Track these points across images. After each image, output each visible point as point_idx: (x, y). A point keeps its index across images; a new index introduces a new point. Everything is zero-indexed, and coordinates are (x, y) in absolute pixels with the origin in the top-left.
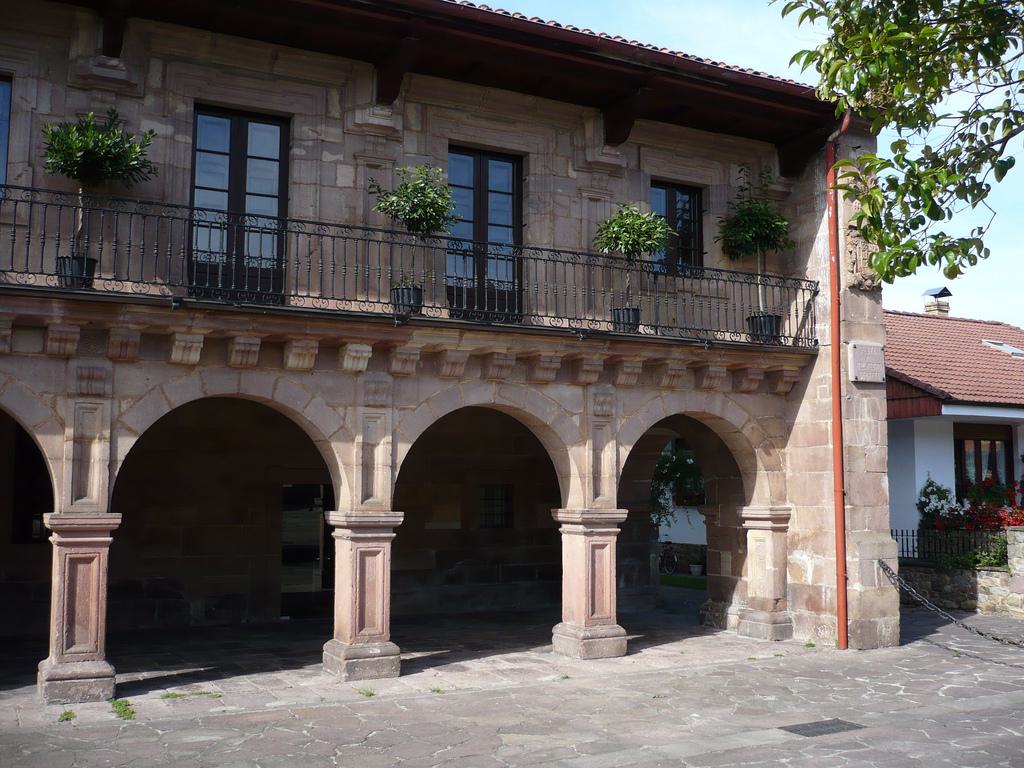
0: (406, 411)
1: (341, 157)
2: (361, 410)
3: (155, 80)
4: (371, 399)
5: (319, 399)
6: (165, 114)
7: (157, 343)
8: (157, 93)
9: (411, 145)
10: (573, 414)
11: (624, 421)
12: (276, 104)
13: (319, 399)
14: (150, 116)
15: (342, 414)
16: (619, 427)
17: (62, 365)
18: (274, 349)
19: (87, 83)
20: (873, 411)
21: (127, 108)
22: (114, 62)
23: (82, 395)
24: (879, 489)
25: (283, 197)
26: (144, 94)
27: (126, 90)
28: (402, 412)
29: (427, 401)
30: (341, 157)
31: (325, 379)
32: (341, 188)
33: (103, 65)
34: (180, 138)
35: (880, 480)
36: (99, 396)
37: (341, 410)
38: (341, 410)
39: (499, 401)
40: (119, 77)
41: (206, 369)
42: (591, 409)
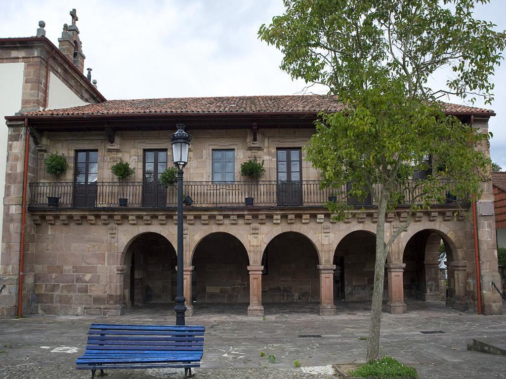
2: (323, 234)
3: (266, 144)
4: (325, 231)
5: (312, 231)
6: (269, 154)
7: (270, 217)
8: (267, 148)
13: (312, 231)
14: (266, 155)
17: (249, 226)
18: (299, 216)
19: (250, 149)
20: (489, 226)
21: (260, 153)
22: (256, 143)
23: (253, 234)
24: (494, 255)
25: (301, 172)
27: (259, 149)
29: (342, 230)
31: (312, 225)
34: (273, 159)
35: (493, 252)
36: (257, 234)
37: (318, 234)
38: (318, 234)
42: (392, 231)
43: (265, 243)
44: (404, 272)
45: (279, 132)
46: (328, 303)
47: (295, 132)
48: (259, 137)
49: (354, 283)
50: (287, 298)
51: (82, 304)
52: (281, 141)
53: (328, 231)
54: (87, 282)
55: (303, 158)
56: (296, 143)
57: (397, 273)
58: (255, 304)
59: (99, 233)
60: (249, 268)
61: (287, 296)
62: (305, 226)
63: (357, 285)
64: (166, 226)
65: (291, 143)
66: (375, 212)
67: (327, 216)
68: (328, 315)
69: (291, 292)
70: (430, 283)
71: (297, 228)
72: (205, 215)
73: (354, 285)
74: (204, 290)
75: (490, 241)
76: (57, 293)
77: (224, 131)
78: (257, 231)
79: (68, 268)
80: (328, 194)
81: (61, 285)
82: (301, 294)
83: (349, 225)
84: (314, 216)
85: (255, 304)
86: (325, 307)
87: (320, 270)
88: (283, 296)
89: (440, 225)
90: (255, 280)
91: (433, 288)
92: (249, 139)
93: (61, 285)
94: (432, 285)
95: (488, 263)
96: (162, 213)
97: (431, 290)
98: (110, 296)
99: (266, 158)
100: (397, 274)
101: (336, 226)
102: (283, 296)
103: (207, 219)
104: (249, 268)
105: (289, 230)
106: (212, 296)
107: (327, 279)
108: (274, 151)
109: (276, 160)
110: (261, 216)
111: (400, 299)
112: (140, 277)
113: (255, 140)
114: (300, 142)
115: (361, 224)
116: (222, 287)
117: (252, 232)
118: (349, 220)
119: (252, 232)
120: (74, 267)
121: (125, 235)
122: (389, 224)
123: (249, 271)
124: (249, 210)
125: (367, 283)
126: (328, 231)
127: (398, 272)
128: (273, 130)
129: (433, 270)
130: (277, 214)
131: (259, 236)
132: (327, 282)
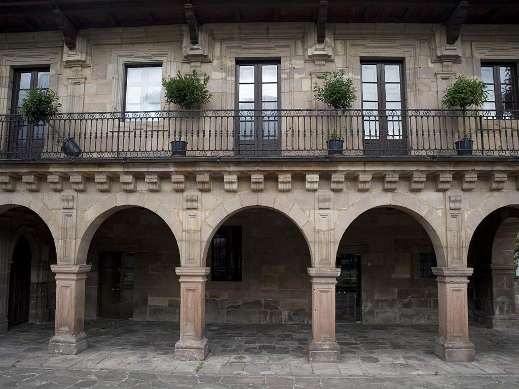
0: (342, 211)
1: (303, 75)
2: (318, 211)
4: (322, 205)
5: (296, 206)
6: (222, 68)
8: (218, 59)
11: (469, 212)
12: (272, 54)
13: (296, 206)
14: (215, 70)
15: (308, 215)
16: (466, 217)
17: (181, 194)
21: (205, 68)
22: (196, 47)
26: (213, 60)
27: (204, 59)
28: (339, 212)
29: (353, 205)
30: (303, 75)
31: (298, 194)
32: (304, 91)
33: (192, 49)
34: (229, 78)
37: (307, 212)
38: (307, 212)
39: (393, 203)
40: (199, 53)
41: (242, 193)
42: (448, 207)
43: (209, 225)
44: (469, 285)
45: (240, 29)
46: (325, 340)
47: (268, 29)
48: (201, 37)
49: (376, 297)
50: (271, 318)
52: (243, 46)
53: (326, 205)
55: (283, 76)
56: (272, 51)
57: (456, 285)
58: (189, 337)
61: (272, 314)
62: (284, 197)
63: (381, 300)
64: (39, 195)
65: (262, 51)
66: (417, 171)
67: (325, 177)
68: (324, 362)
69: (278, 309)
70: (499, 299)
71: (270, 199)
72: (101, 173)
73: (376, 299)
74: (145, 302)
77: (142, 29)
78: (195, 205)
80: (325, 136)
82: (292, 312)
83: (365, 195)
84: (299, 178)
85: (189, 337)
86: (320, 347)
87: (311, 277)
88: (265, 313)
90: (191, 293)
91: (506, 308)
92: (186, 42)
94: (504, 303)
96: (27, 170)
97: (501, 310)
99: (216, 75)
101: (341, 196)
102: (265, 313)
103: (105, 181)
105: (254, 204)
106: (157, 310)
107: (324, 295)
108: (231, 63)
109: (233, 79)
110: (201, 176)
111: (461, 334)
112: (41, 281)
113: (194, 41)
114: (280, 49)
115: (390, 195)
116: (172, 298)
117: (186, 205)
118: (367, 186)
119: (186, 205)
122: (441, 194)
123: (179, 277)
124: (177, 164)
125: (396, 297)
126: (326, 205)
127: (457, 283)
128: (228, 26)
129: (505, 279)
130: (230, 173)
131: (199, 212)
132: (324, 299)
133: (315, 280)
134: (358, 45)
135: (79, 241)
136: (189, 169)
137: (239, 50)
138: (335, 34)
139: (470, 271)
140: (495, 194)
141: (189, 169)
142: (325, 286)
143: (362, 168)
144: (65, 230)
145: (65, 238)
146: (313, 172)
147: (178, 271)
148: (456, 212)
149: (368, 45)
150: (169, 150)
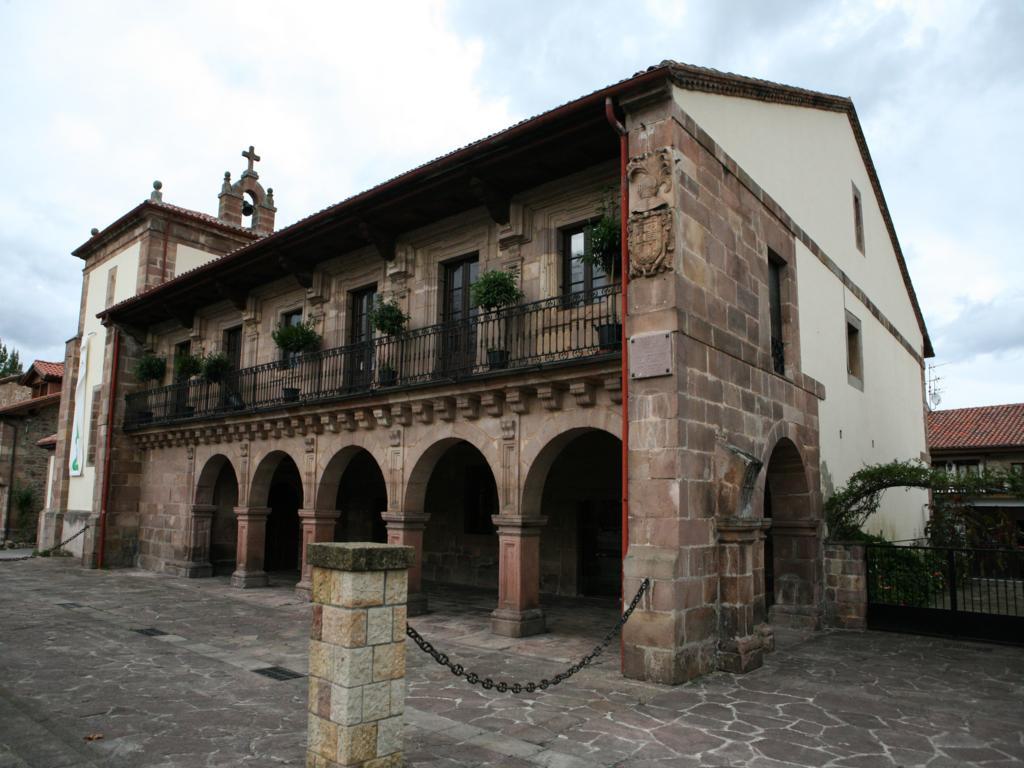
9: (419, 275)
10: (494, 440)
14: (331, 309)
24: (667, 499)
35: (667, 489)
51: (166, 557)
53: (397, 441)
54: (172, 528)
59: (180, 456)
60: (384, 515)
66: (437, 398)
70: (784, 578)
75: (658, 454)
76: (152, 541)
79: (160, 507)
81: (156, 529)
89: (608, 416)
91: (795, 594)
93: (156, 529)
95: (651, 521)
97: (787, 597)
98: (186, 548)
100: (509, 539)
104: (495, 520)
120: (165, 507)
121: (205, 453)
124: (289, 410)
126: (397, 441)
129: (795, 544)
133: (389, 526)
134: (436, 249)
135: (250, 485)
136: (593, 373)
137: (349, 283)
138: (412, 244)
139: (545, 521)
140: (556, 414)
141: (593, 373)
142: (395, 532)
143: (436, 395)
144: (243, 475)
145: (243, 482)
146: (377, 407)
147: (301, 512)
148: (510, 442)
149: (443, 246)
150: (593, 346)
